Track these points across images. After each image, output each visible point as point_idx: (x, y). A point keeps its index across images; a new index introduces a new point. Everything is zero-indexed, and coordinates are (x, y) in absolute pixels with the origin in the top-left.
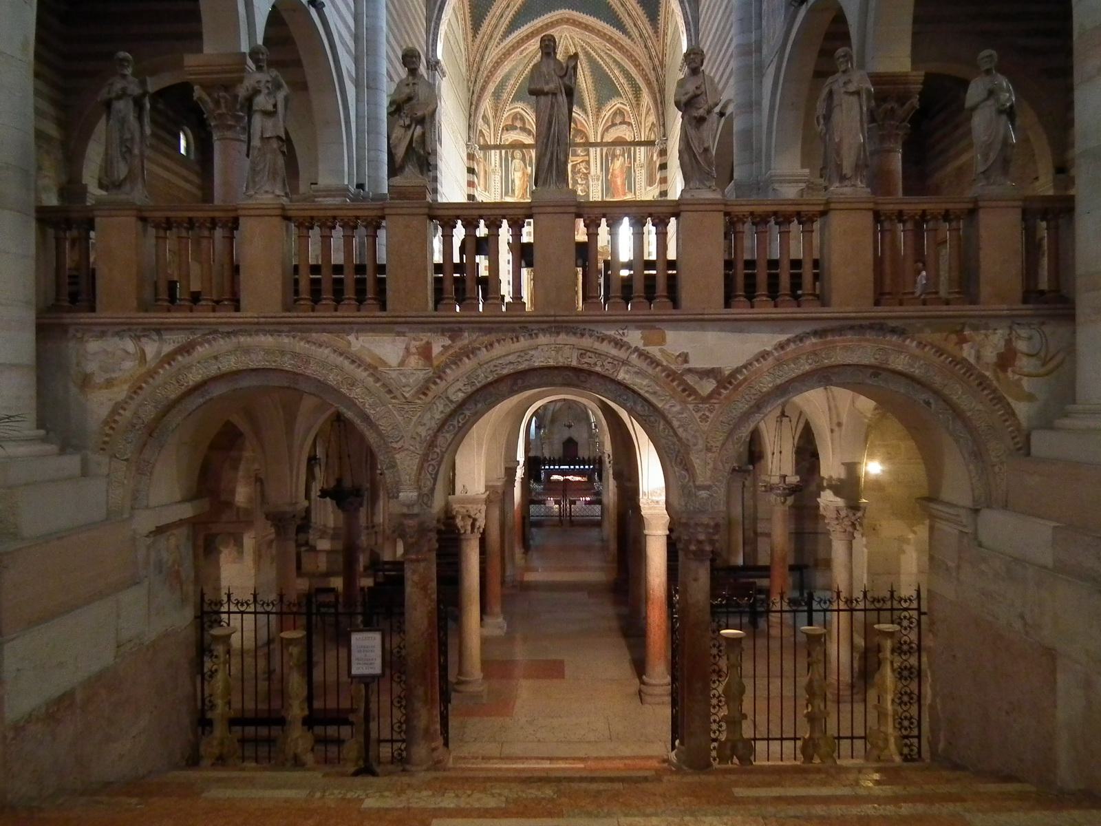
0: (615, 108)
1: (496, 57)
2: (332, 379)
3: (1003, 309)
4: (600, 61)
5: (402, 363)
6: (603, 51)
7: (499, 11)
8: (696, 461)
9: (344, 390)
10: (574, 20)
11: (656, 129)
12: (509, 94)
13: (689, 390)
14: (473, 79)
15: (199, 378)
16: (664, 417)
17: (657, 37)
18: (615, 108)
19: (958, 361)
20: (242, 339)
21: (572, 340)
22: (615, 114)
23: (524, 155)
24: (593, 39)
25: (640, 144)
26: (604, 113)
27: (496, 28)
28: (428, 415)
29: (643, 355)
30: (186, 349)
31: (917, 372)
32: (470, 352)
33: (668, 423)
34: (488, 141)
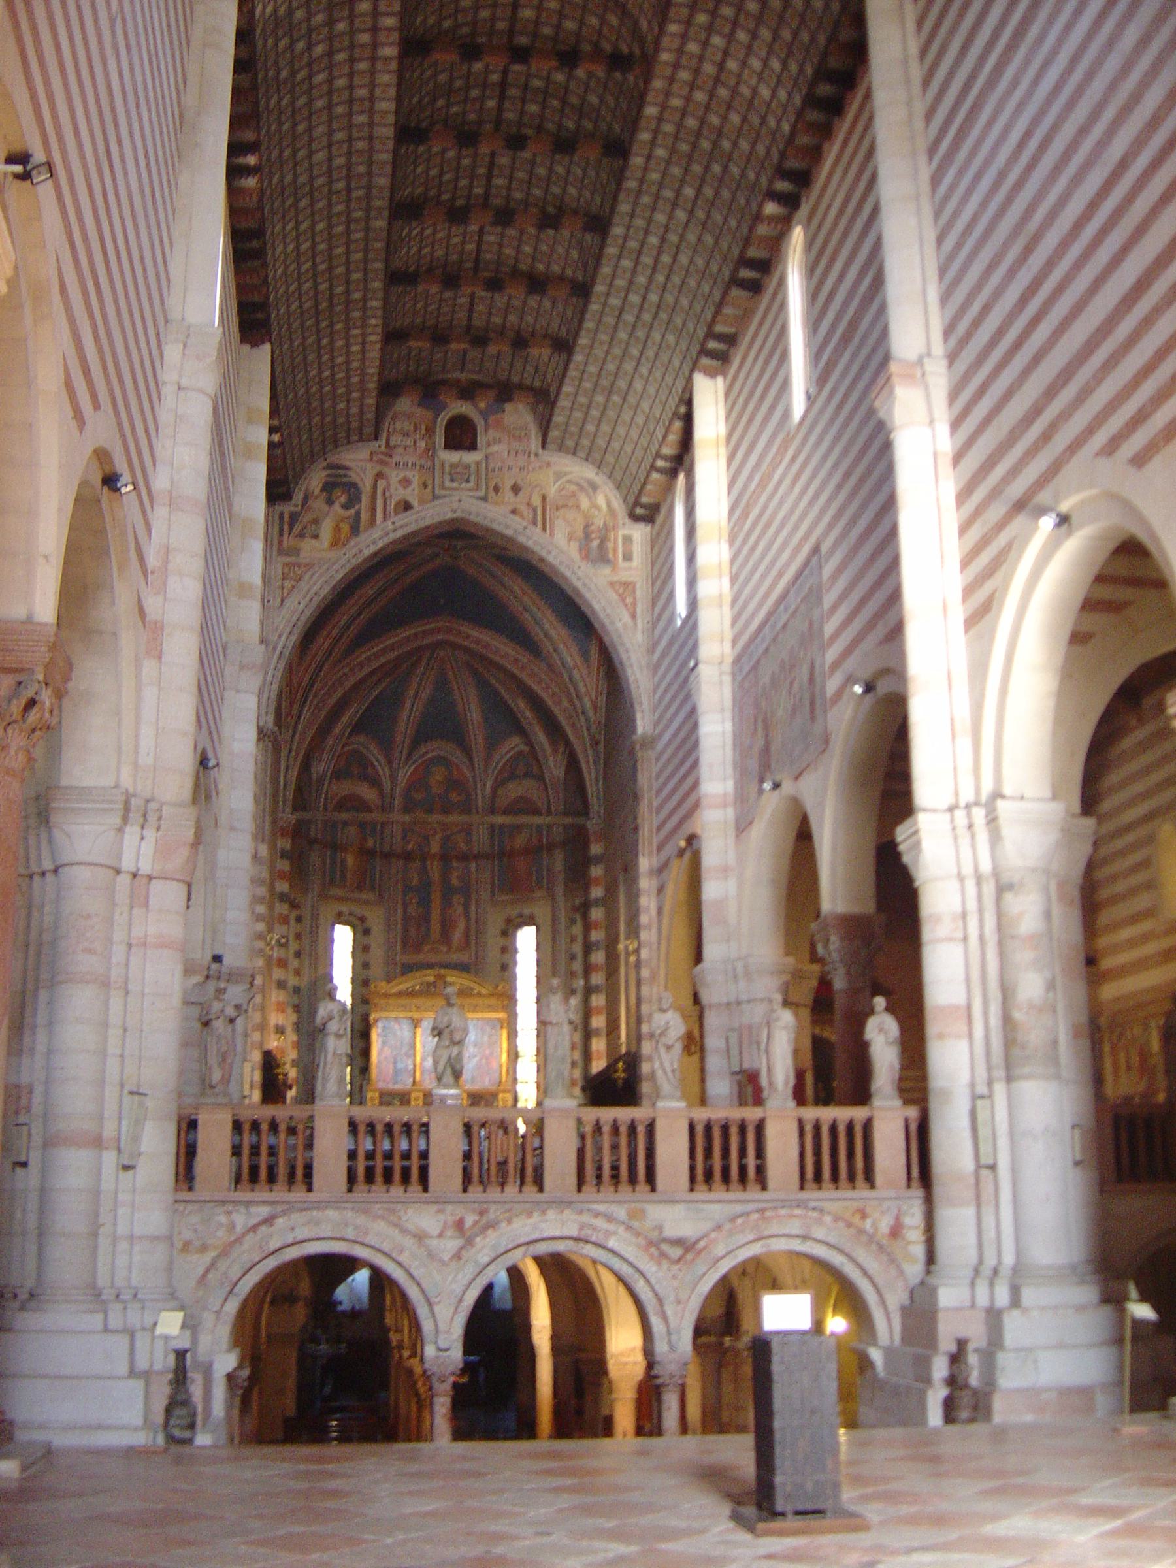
2: (386, 1246)
3: (892, 1194)
5: (441, 1235)
8: (670, 1310)
9: (394, 1255)
13: (663, 1255)
14: (295, 712)
15: (278, 1245)
16: (645, 1277)
17: (588, 667)
19: (861, 1231)
20: (315, 1213)
21: (574, 1217)
26: (496, 757)
28: (460, 1276)
29: (629, 1228)
30: (269, 1221)
31: (832, 1239)
32: (492, 1225)
33: (648, 1281)
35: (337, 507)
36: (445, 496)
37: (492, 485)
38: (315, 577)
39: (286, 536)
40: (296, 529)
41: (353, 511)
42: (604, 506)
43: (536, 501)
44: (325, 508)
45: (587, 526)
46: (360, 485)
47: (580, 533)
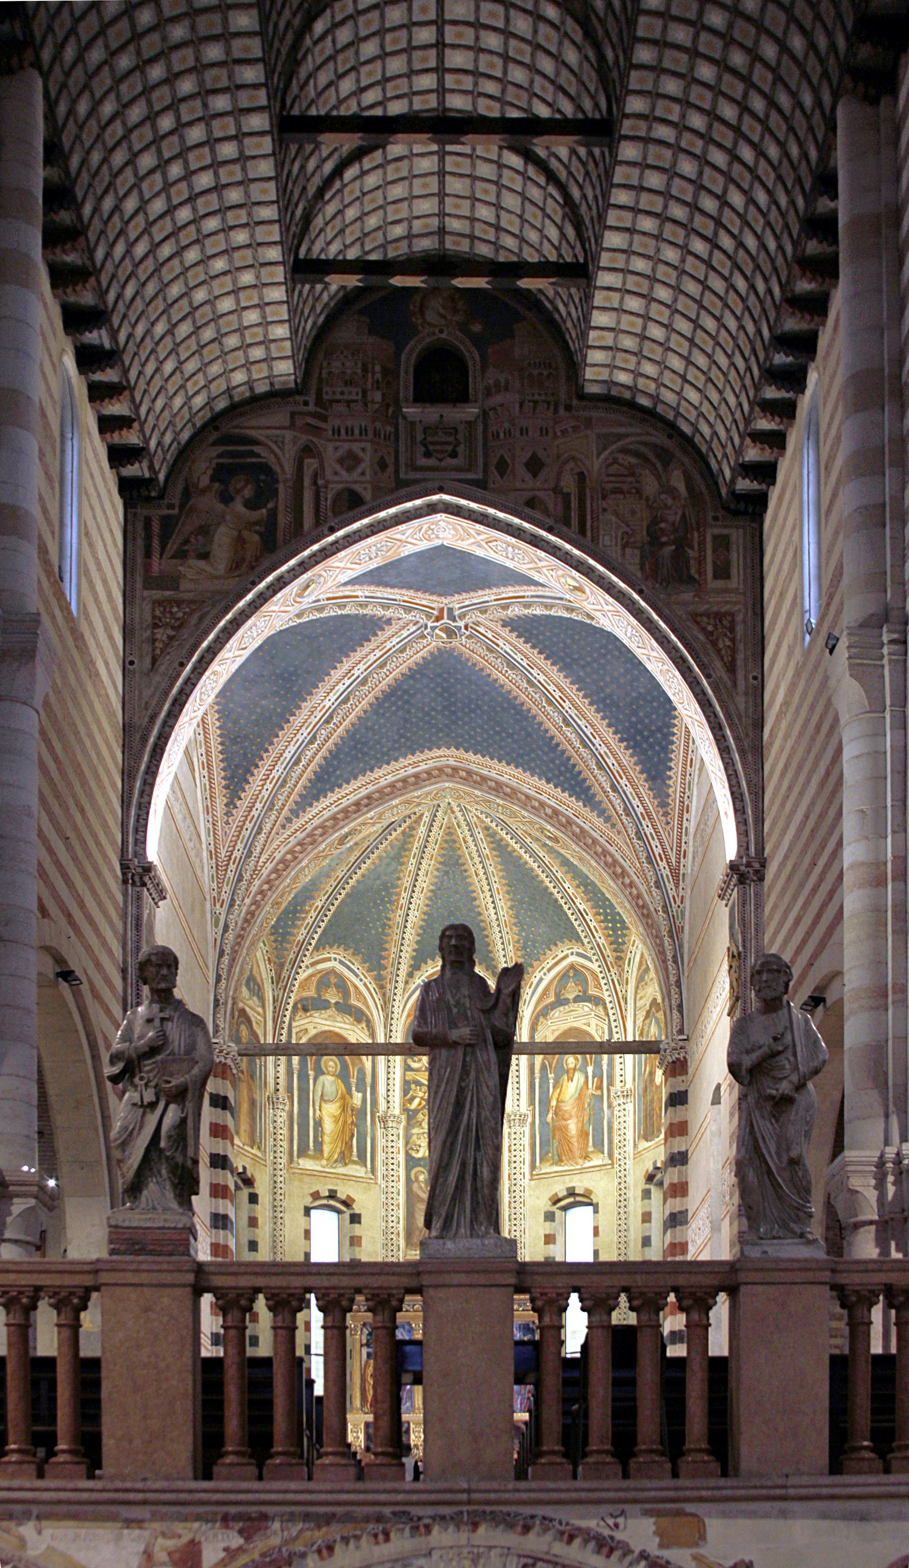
0: (564, 963)
1: (283, 850)
4: (530, 861)
6: (537, 840)
7: (292, 749)
10: (469, 773)
11: (661, 1015)
12: (311, 931)
18: (564, 963)
22: (564, 977)
23: (345, 1067)
24: (514, 815)
25: (624, 1048)
26: (538, 975)
27: (282, 786)
34: (260, 1033)
35: (238, 506)
36: (416, 482)
37: (494, 461)
38: (206, 622)
39: (155, 559)
40: (172, 547)
41: (264, 511)
42: (682, 488)
43: (569, 484)
44: (220, 507)
45: (655, 522)
46: (277, 468)
47: (642, 536)
